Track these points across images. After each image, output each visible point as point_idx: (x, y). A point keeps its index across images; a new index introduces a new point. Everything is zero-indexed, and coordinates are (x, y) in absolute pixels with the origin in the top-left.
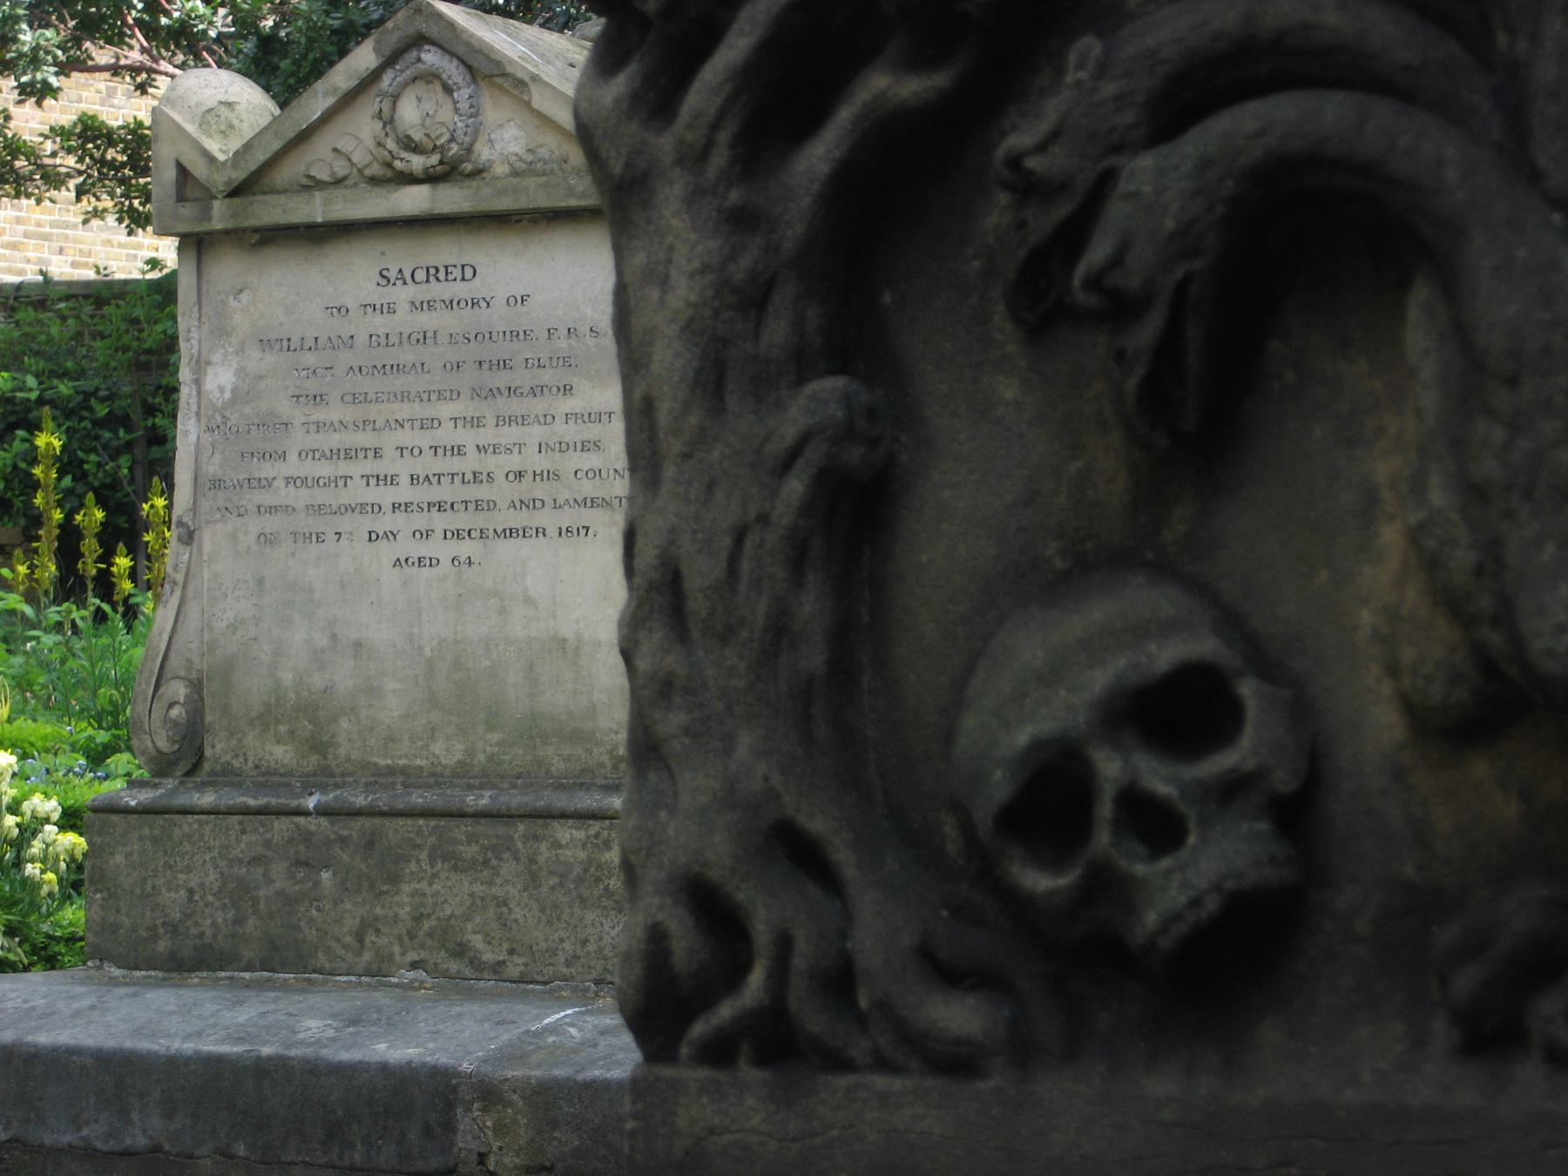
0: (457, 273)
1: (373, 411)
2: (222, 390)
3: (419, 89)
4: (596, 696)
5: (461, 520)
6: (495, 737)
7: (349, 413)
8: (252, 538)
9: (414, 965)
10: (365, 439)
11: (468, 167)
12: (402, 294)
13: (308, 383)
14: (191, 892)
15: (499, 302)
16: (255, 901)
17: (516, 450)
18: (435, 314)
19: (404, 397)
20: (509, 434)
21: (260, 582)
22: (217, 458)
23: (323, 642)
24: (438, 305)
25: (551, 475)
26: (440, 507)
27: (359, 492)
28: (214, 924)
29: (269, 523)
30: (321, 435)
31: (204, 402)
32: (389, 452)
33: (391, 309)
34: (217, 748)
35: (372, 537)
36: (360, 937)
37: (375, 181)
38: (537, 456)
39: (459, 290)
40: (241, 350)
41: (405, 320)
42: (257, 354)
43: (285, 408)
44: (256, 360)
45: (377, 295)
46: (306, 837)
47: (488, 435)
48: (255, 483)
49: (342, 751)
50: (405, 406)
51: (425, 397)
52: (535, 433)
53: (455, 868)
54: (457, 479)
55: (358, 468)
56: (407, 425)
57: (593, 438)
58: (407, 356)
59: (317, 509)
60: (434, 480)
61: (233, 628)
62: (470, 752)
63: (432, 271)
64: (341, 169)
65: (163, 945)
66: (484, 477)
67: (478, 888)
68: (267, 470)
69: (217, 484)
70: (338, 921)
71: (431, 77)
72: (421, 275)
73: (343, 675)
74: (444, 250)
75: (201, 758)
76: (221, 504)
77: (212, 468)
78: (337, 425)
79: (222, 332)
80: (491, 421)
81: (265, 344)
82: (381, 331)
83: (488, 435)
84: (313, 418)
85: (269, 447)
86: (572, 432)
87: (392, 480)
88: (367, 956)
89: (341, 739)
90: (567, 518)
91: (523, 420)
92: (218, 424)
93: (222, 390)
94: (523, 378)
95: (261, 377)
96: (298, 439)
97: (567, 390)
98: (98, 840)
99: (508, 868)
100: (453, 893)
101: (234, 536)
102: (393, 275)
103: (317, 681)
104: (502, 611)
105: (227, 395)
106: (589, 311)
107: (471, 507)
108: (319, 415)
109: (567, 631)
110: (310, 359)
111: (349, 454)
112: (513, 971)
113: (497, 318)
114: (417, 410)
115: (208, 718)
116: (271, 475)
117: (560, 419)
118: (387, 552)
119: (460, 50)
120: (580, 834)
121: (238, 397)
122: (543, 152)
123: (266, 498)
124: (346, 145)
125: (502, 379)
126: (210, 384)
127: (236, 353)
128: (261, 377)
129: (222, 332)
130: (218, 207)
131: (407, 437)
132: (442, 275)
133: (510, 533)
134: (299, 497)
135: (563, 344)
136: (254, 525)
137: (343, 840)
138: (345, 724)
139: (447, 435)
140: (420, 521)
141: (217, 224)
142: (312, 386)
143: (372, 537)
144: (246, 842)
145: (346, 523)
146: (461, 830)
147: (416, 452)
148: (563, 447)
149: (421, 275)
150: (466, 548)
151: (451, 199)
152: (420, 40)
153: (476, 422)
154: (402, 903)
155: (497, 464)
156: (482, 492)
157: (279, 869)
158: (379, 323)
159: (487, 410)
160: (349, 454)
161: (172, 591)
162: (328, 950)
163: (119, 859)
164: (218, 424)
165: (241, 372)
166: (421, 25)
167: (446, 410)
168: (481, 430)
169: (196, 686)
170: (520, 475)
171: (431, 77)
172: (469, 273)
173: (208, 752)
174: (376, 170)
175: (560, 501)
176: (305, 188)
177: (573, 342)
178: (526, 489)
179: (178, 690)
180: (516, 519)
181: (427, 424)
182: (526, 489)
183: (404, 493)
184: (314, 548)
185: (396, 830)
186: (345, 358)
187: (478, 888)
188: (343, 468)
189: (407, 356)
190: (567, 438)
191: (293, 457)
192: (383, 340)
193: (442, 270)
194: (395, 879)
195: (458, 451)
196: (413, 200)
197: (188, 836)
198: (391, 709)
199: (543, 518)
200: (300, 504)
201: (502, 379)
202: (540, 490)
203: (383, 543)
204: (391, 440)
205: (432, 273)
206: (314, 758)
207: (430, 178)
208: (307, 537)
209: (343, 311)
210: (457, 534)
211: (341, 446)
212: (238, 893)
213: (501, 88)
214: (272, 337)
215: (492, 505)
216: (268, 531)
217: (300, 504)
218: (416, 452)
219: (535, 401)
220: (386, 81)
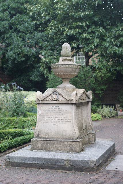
3: (55, 95)
20: (61, 117)
21: (43, 125)
23: (48, 129)
27: (50, 120)
29: (44, 122)
35: (51, 123)
37: (52, 100)
40: (42, 110)
41: (54, 109)
42: (43, 111)
45: (52, 108)
64: (49, 99)
65: (37, 149)
68: (44, 118)
71: (56, 94)
73: (49, 132)
74: (56, 105)
75: (39, 136)
77: (40, 118)
81: (44, 110)
86: (65, 117)
91: (62, 116)
92: (40, 115)
96: (46, 117)
99: (61, 144)
100: (58, 146)
103: (47, 132)
108: (48, 115)
109: (65, 129)
111: (50, 118)
113: (60, 109)
121: (42, 114)
124: (50, 98)
126: (40, 112)
134: (46, 120)
139: (56, 117)
140: (55, 122)
141: (41, 102)
142: (47, 113)
143: (51, 123)
144: (43, 142)
150: (58, 124)
152: (55, 92)
153: (59, 116)
154: (54, 146)
156: (59, 120)
160: (50, 118)
164: (40, 115)
165: (42, 112)
166: (55, 91)
171: (56, 94)
179: (37, 132)
180: (62, 122)
181: (55, 116)
182: (62, 120)
195: (57, 118)
198: (53, 134)
207: (56, 101)
220: (53, 94)
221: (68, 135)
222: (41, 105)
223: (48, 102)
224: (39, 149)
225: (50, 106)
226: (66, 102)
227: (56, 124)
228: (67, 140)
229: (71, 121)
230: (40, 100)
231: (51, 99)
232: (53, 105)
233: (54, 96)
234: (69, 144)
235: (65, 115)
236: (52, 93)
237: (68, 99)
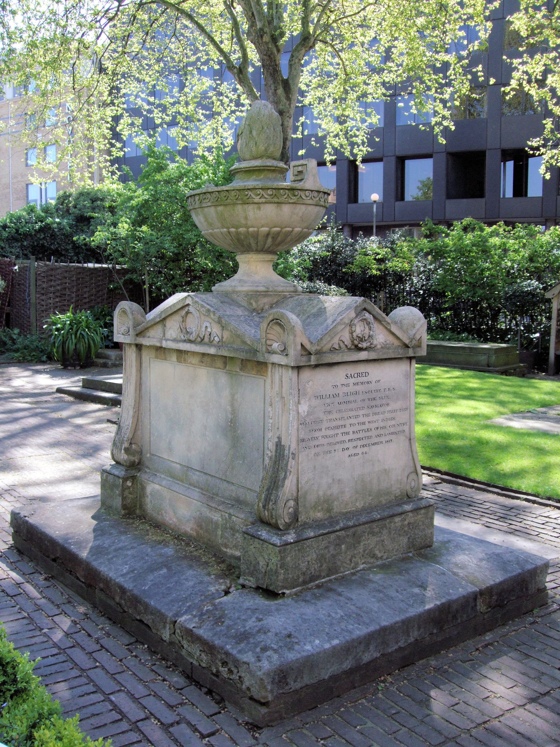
1: (345, 415)
2: (304, 412)
4: (392, 482)
6: (370, 498)
8: (312, 455)
9: (363, 563)
14: (308, 562)
16: (325, 559)
21: (315, 467)
23: (330, 481)
25: (385, 427)
26: (359, 439)
27: (340, 438)
28: (315, 569)
29: (317, 450)
32: (348, 426)
33: (348, 385)
34: (302, 518)
36: (351, 561)
41: (352, 388)
42: (314, 400)
43: (322, 416)
44: (315, 402)
45: (345, 381)
46: (339, 537)
47: (370, 418)
49: (335, 511)
51: (357, 409)
52: (381, 417)
53: (373, 535)
58: (351, 398)
59: (329, 444)
61: (307, 482)
62: (365, 504)
65: (301, 580)
67: (378, 539)
68: (317, 434)
69: (303, 440)
70: (346, 558)
72: (356, 376)
73: (335, 490)
74: (361, 368)
76: (304, 446)
77: (301, 436)
79: (305, 395)
80: (371, 415)
83: (370, 418)
85: (317, 428)
86: (388, 415)
87: (348, 433)
88: (352, 565)
89: (335, 507)
90: (387, 438)
93: (304, 412)
94: (378, 402)
96: (325, 424)
97: (388, 405)
98: (283, 555)
99: (385, 532)
101: (308, 455)
102: (349, 375)
103: (329, 493)
104: (373, 465)
108: (330, 417)
109: (387, 467)
110: (328, 401)
111: (337, 427)
112: (385, 557)
113: (373, 387)
115: (300, 510)
118: (347, 453)
120: (400, 519)
121: (309, 413)
122: (388, 342)
123: (316, 443)
125: (374, 403)
129: (305, 395)
133: (374, 444)
135: (387, 393)
136: (313, 451)
137: (348, 536)
138: (336, 503)
139: (361, 419)
140: (355, 444)
141: (313, 363)
142: (329, 408)
143: (343, 450)
144: (324, 544)
146: (374, 525)
149: (356, 376)
150: (365, 449)
151: (372, 355)
153: (367, 415)
155: (373, 426)
157: (332, 548)
158: (345, 389)
159: (370, 411)
160: (337, 427)
162: (344, 567)
163: (289, 558)
167: (361, 412)
169: (296, 500)
170: (377, 428)
173: (300, 520)
179: (292, 503)
181: (357, 417)
183: (351, 436)
184: (329, 455)
185: (360, 529)
186: (337, 400)
187: (378, 539)
188: (336, 431)
189: (351, 398)
191: (323, 430)
194: (359, 542)
195: (364, 423)
196: (363, 355)
197: (308, 546)
198: (347, 496)
199: (383, 439)
200: (325, 444)
201: (374, 403)
202: (382, 432)
205: (359, 375)
206: (328, 514)
207: (366, 349)
210: (363, 446)
212: (321, 558)
213: (382, 324)
217: (325, 444)
221: (396, 490)
224: (308, 577)
226: (401, 352)
227: (359, 450)
228: (400, 510)
234: (406, 522)
235: (389, 408)
237: (407, 342)
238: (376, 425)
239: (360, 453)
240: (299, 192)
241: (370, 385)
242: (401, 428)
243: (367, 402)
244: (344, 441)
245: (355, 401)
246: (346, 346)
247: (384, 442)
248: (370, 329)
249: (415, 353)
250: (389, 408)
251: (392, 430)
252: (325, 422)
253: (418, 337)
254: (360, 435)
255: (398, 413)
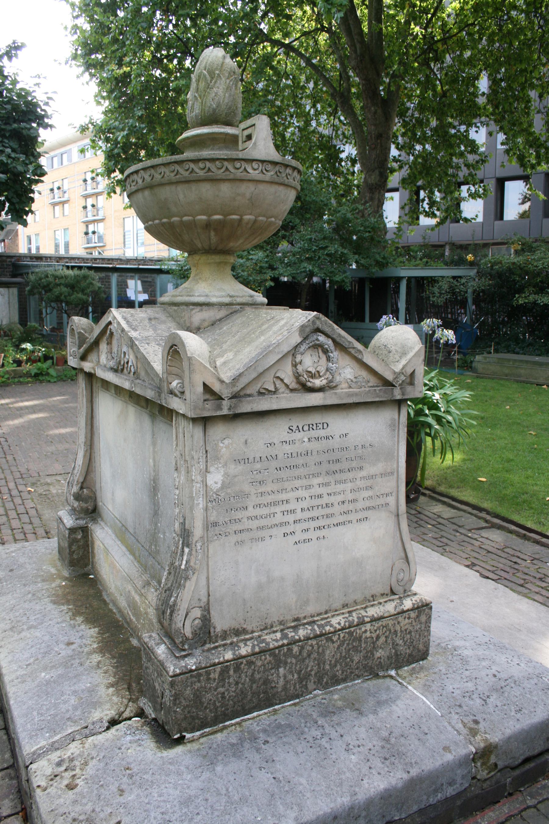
0: (321, 426)
1: (286, 485)
2: (216, 483)
5: (321, 523)
7: (275, 487)
10: (284, 496)
11: (334, 385)
12: (298, 436)
13: (257, 476)
15: (337, 437)
17: (342, 493)
18: (311, 443)
19: (299, 478)
22: (215, 513)
24: (313, 440)
25: (354, 501)
26: (313, 519)
27: (279, 518)
29: (239, 537)
30: (263, 497)
31: (208, 489)
37: (292, 390)
38: (350, 494)
39: (322, 433)
40: (225, 465)
42: (233, 466)
43: (247, 488)
44: (233, 469)
45: (287, 437)
48: (233, 521)
50: (300, 481)
52: (349, 486)
54: (320, 507)
55: (278, 509)
56: (300, 489)
57: (369, 485)
58: (300, 461)
59: (262, 528)
60: (311, 509)
63: (311, 426)
66: (330, 505)
68: (239, 515)
69: (215, 524)
72: (306, 428)
74: (316, 418)
76: (218, 533)
77: (213, 518)
78: (270, 492)
80: (333, 483)
81: (238, 461)
82: (289, 452)
84: (260, 491)
85: (239, 505)
87: (293, 511)
90: (360, 515)
91: (345, 481)
94: (345, 465)
95: (235, 476)
97: (361, 468)
102: (294, 428)
105: (219, 485)
106: (369, 438)
107: (325, 517)
110: (258, 466)
111: (275, 504)
113: (335, 443)
114: (305, 482)
116: (240, 517)
117: (358, 479)
118: (291, 539)
119: (334, 336)
121: (224, 486)
125: (337, 467)
127: (223, 467)
128: (235, 476)
129: (217, 458)
130: (226, 404)
131: (301, 493)
132: (314, 427)
135: (360, 451)
136: (233, 538)
140: (305, 525)
141: (225, 412)
142: (259, 477)
145: (274, 531)
147: (304, 499)
148: (359, 489)
149: (306, 428)
153: (327, 484)
158: (288, 448)
161: (194, 573)
165: (226, 475)
167: (316, 481)
168: (329, 487)
170: (343, 502)
172: (325, 425)
174: (293, 385)
175: (358, 509)
176: (260, 393)
177: (364, 450)
178: (346, 507)
180: (341, 519)
181: (308, 487)
182: (346, 507)
183: (299, 515)
184: (261, 544)
186: (274, 464)
188: (273, 509)
189: (300, 461)
190: (361, 486)
191: (250, 508)
192: (290, 456)
193: (315, 425)
199: (352, 517)
200: (254, 527)
201: (337, 467)
203: (290, 537)
204: (291, 495)
207: (321, 389)
208: (257, 540)
209: (273, 444)
210: (319, 528)
211: (272, 501)
214: (240, 458)
215: (332, 515)
216: (239, 540)
217: (254, 527)
218: (304, 499)
219: (349, 474)
220: (303, 348)
222: (218, 431)
223: (275, 407)
225: (277, 431)
229: (391, 500)
230: (226, 393)
231: (289, 379)
232: (297, 421)
233: (309, 361)
235: (363, 473)
236: (299, 340)
237: (390, 377)
238: (340, 498)
239: (314, 539)
240: (243, 163)
241: (331, 441)
242: (381, 501)
243: (325, 466)
244: (287, 523)
245: (305, 465)
246: (287, 386)
247: (354, 521)
248: (328, 359)
249: (403, 394)
250: (363, 473)
251: (368, 504)
252: (253, 497)
253: (409, 371)
254: (315, 513)
255: (379, 480)
